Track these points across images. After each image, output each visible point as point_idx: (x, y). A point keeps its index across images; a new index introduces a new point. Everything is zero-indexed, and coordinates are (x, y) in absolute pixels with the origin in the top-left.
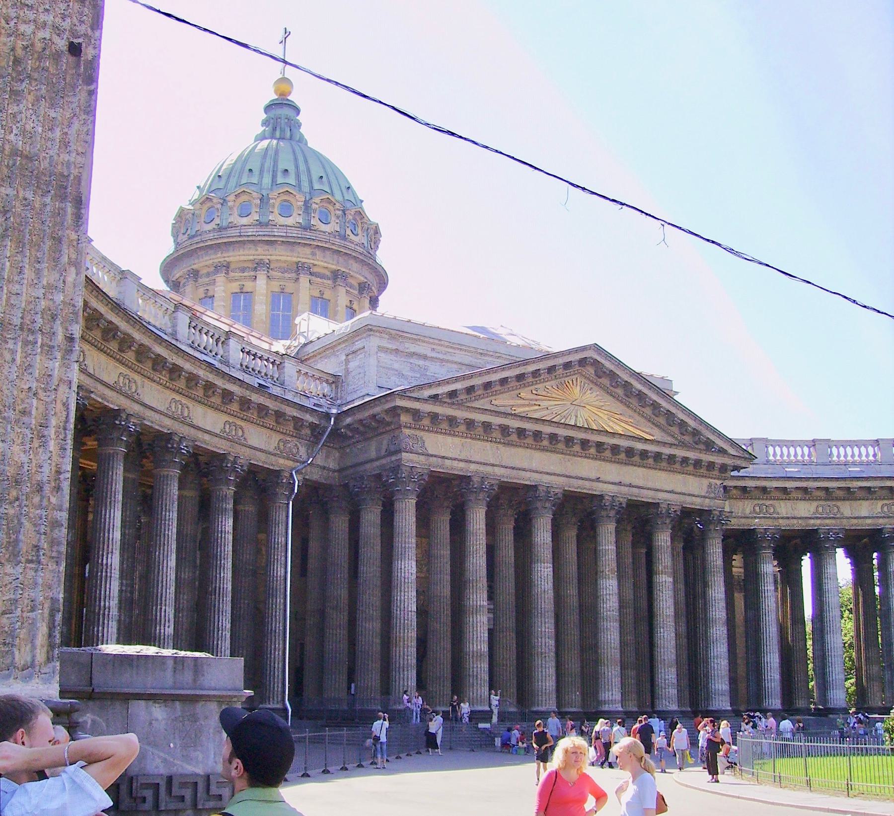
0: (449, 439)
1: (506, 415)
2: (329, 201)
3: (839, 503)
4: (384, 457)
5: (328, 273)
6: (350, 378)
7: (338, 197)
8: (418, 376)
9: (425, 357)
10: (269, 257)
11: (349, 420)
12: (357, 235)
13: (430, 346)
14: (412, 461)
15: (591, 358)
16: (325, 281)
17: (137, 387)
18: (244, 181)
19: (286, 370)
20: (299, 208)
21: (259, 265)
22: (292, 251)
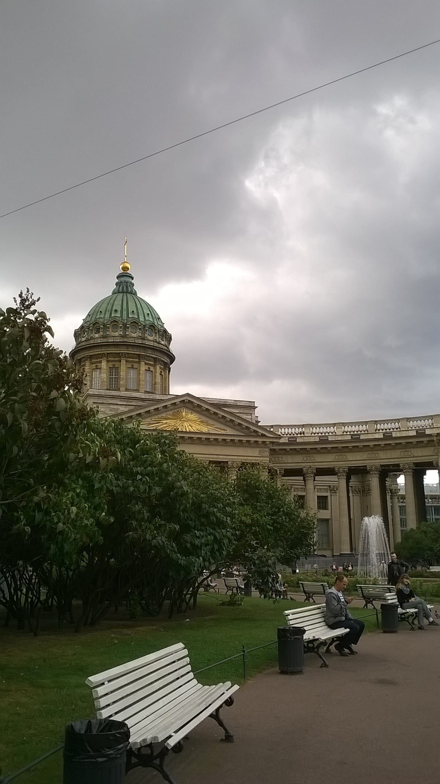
2: (135, 322)
3: (346, 454)
7: (142, 319)
8: (114, 413)
9: (117, 404)
10: (107, 352)
12: (152, 336)
13: (119, 399)
15: (187, 400)
16: (135, 360)
18: (98, 317)
20: (121, 327)
21: (101, 356)
22: (117, 348)
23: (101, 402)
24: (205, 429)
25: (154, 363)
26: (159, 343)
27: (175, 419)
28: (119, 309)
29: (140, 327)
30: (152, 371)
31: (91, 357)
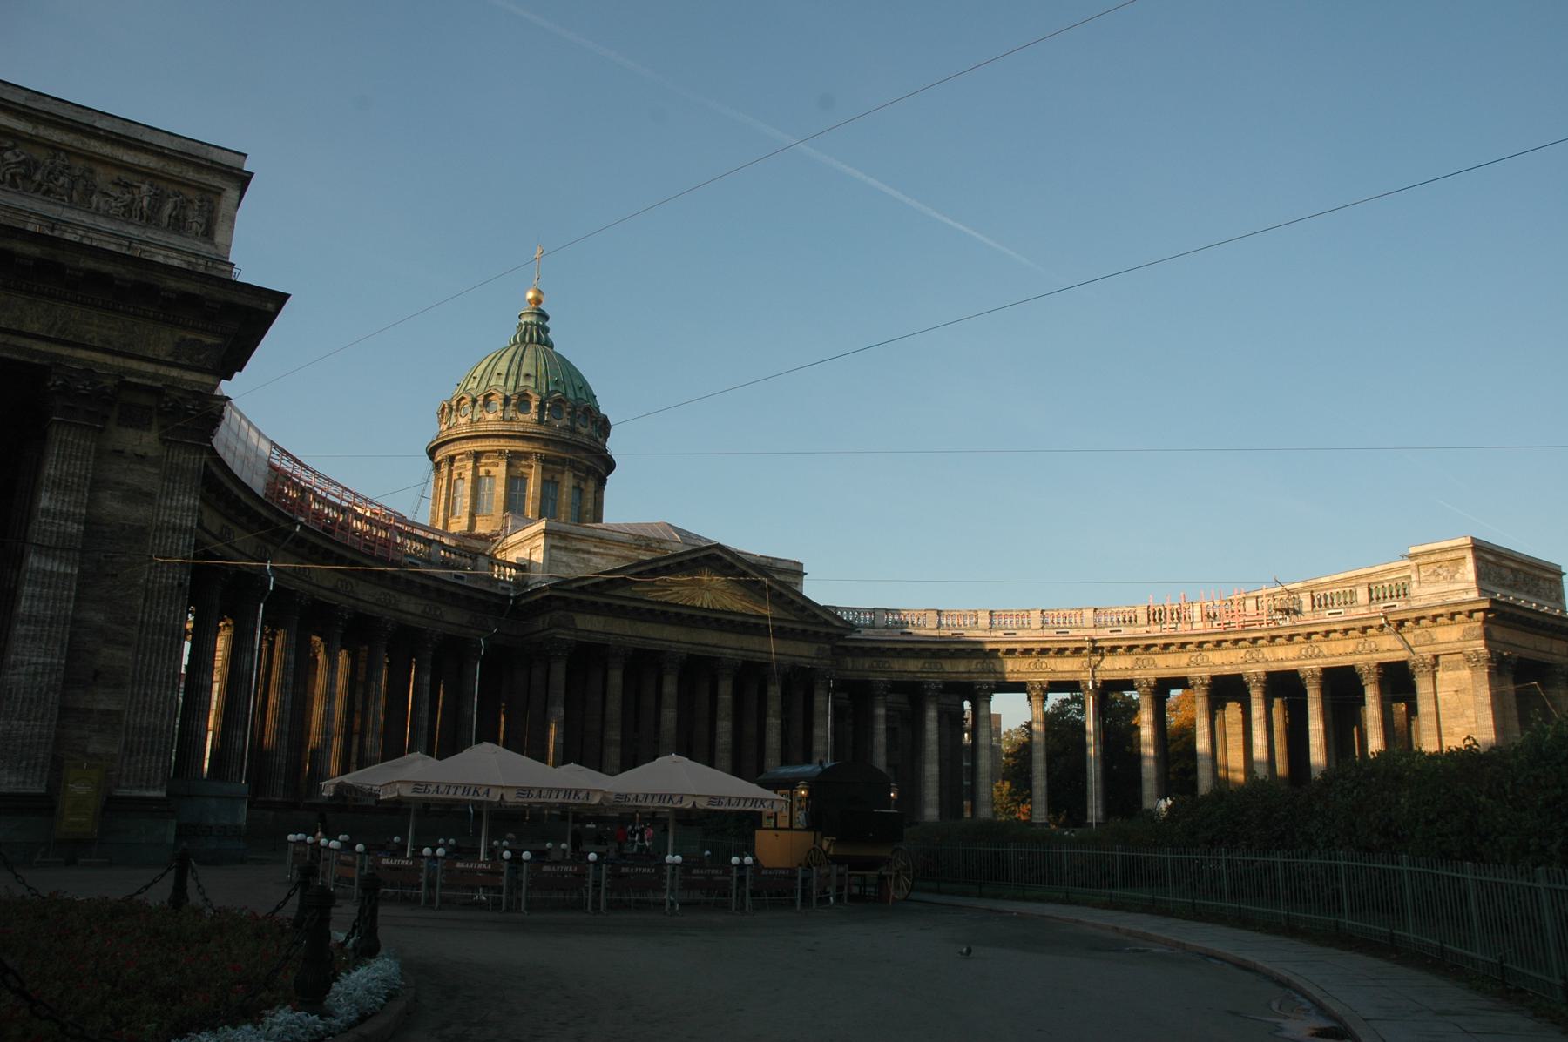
0: (595, 618)
1: (641, 600)
2: (559, 400)
3: (943, 661)
4: (547, 630)
5: (559, 460)
6: (532, 566)
7: (571, 395)
8: (582, 566)
9: (589, 552)
10: (509, 448)
11: (523, 601)
12: (586, 427)
14: (564, 634)
17: (352, 587)
19: (479, 563)
23: (562, 544)
24: (738, 606)
25: (587, 475)
26: (596, 440)
27: (692, 586)
28: (533, 373)
29: (568, 410)
30: (581, 491)
31: (477, 456)
